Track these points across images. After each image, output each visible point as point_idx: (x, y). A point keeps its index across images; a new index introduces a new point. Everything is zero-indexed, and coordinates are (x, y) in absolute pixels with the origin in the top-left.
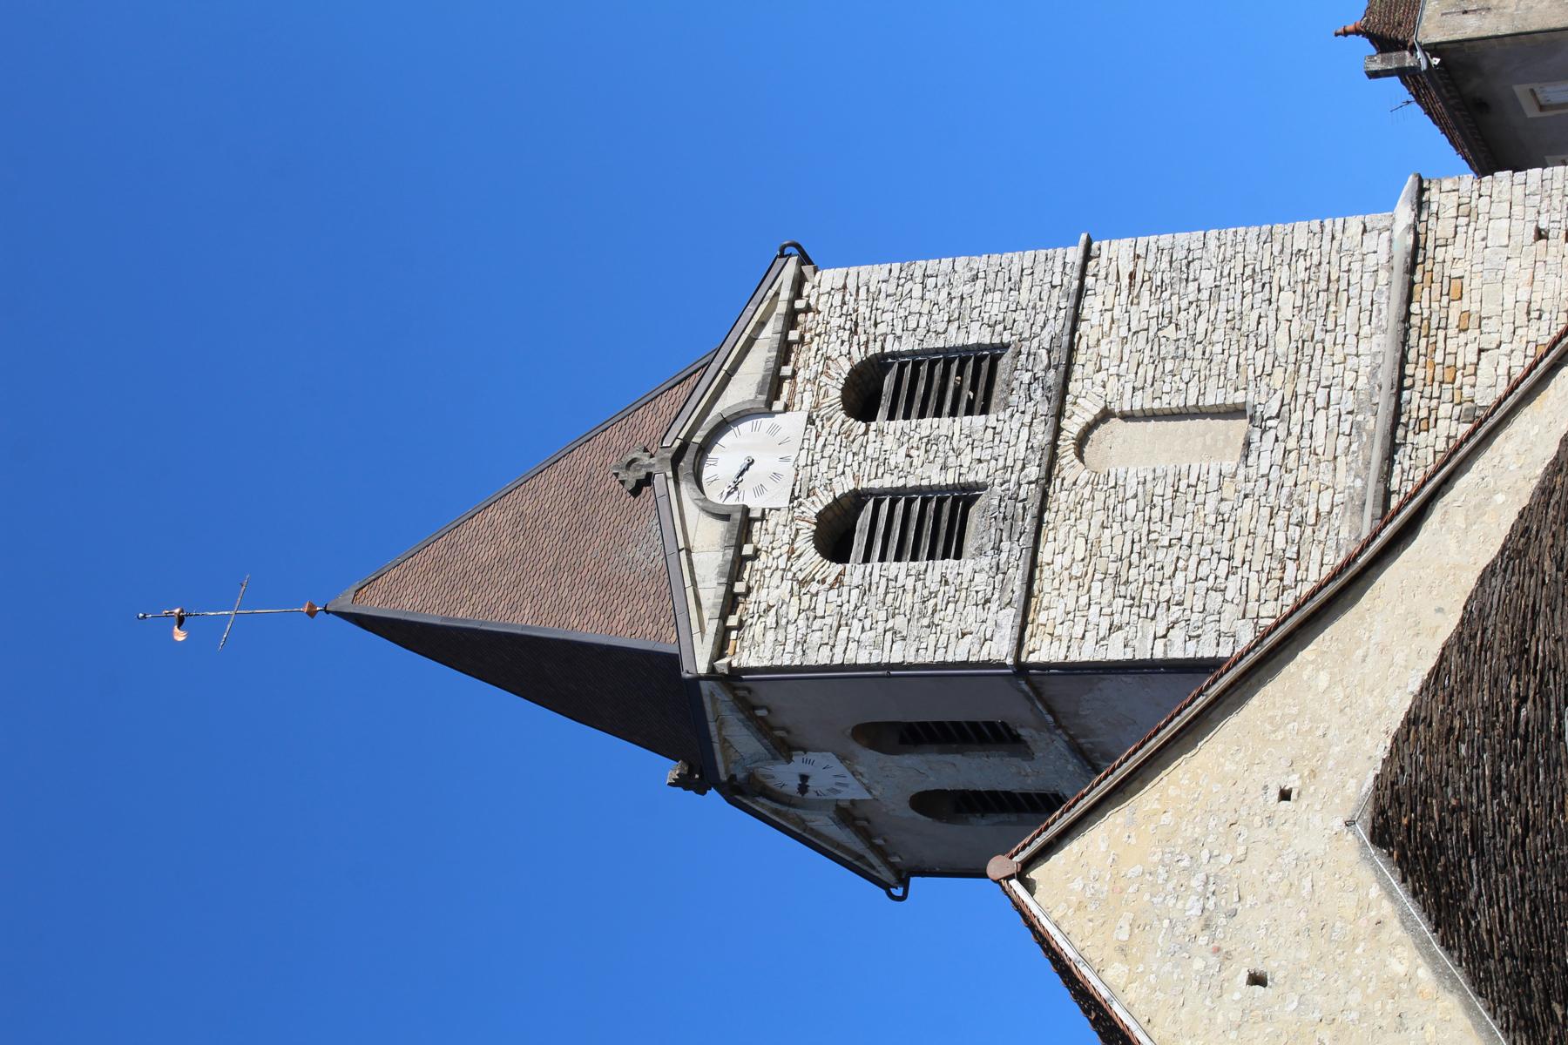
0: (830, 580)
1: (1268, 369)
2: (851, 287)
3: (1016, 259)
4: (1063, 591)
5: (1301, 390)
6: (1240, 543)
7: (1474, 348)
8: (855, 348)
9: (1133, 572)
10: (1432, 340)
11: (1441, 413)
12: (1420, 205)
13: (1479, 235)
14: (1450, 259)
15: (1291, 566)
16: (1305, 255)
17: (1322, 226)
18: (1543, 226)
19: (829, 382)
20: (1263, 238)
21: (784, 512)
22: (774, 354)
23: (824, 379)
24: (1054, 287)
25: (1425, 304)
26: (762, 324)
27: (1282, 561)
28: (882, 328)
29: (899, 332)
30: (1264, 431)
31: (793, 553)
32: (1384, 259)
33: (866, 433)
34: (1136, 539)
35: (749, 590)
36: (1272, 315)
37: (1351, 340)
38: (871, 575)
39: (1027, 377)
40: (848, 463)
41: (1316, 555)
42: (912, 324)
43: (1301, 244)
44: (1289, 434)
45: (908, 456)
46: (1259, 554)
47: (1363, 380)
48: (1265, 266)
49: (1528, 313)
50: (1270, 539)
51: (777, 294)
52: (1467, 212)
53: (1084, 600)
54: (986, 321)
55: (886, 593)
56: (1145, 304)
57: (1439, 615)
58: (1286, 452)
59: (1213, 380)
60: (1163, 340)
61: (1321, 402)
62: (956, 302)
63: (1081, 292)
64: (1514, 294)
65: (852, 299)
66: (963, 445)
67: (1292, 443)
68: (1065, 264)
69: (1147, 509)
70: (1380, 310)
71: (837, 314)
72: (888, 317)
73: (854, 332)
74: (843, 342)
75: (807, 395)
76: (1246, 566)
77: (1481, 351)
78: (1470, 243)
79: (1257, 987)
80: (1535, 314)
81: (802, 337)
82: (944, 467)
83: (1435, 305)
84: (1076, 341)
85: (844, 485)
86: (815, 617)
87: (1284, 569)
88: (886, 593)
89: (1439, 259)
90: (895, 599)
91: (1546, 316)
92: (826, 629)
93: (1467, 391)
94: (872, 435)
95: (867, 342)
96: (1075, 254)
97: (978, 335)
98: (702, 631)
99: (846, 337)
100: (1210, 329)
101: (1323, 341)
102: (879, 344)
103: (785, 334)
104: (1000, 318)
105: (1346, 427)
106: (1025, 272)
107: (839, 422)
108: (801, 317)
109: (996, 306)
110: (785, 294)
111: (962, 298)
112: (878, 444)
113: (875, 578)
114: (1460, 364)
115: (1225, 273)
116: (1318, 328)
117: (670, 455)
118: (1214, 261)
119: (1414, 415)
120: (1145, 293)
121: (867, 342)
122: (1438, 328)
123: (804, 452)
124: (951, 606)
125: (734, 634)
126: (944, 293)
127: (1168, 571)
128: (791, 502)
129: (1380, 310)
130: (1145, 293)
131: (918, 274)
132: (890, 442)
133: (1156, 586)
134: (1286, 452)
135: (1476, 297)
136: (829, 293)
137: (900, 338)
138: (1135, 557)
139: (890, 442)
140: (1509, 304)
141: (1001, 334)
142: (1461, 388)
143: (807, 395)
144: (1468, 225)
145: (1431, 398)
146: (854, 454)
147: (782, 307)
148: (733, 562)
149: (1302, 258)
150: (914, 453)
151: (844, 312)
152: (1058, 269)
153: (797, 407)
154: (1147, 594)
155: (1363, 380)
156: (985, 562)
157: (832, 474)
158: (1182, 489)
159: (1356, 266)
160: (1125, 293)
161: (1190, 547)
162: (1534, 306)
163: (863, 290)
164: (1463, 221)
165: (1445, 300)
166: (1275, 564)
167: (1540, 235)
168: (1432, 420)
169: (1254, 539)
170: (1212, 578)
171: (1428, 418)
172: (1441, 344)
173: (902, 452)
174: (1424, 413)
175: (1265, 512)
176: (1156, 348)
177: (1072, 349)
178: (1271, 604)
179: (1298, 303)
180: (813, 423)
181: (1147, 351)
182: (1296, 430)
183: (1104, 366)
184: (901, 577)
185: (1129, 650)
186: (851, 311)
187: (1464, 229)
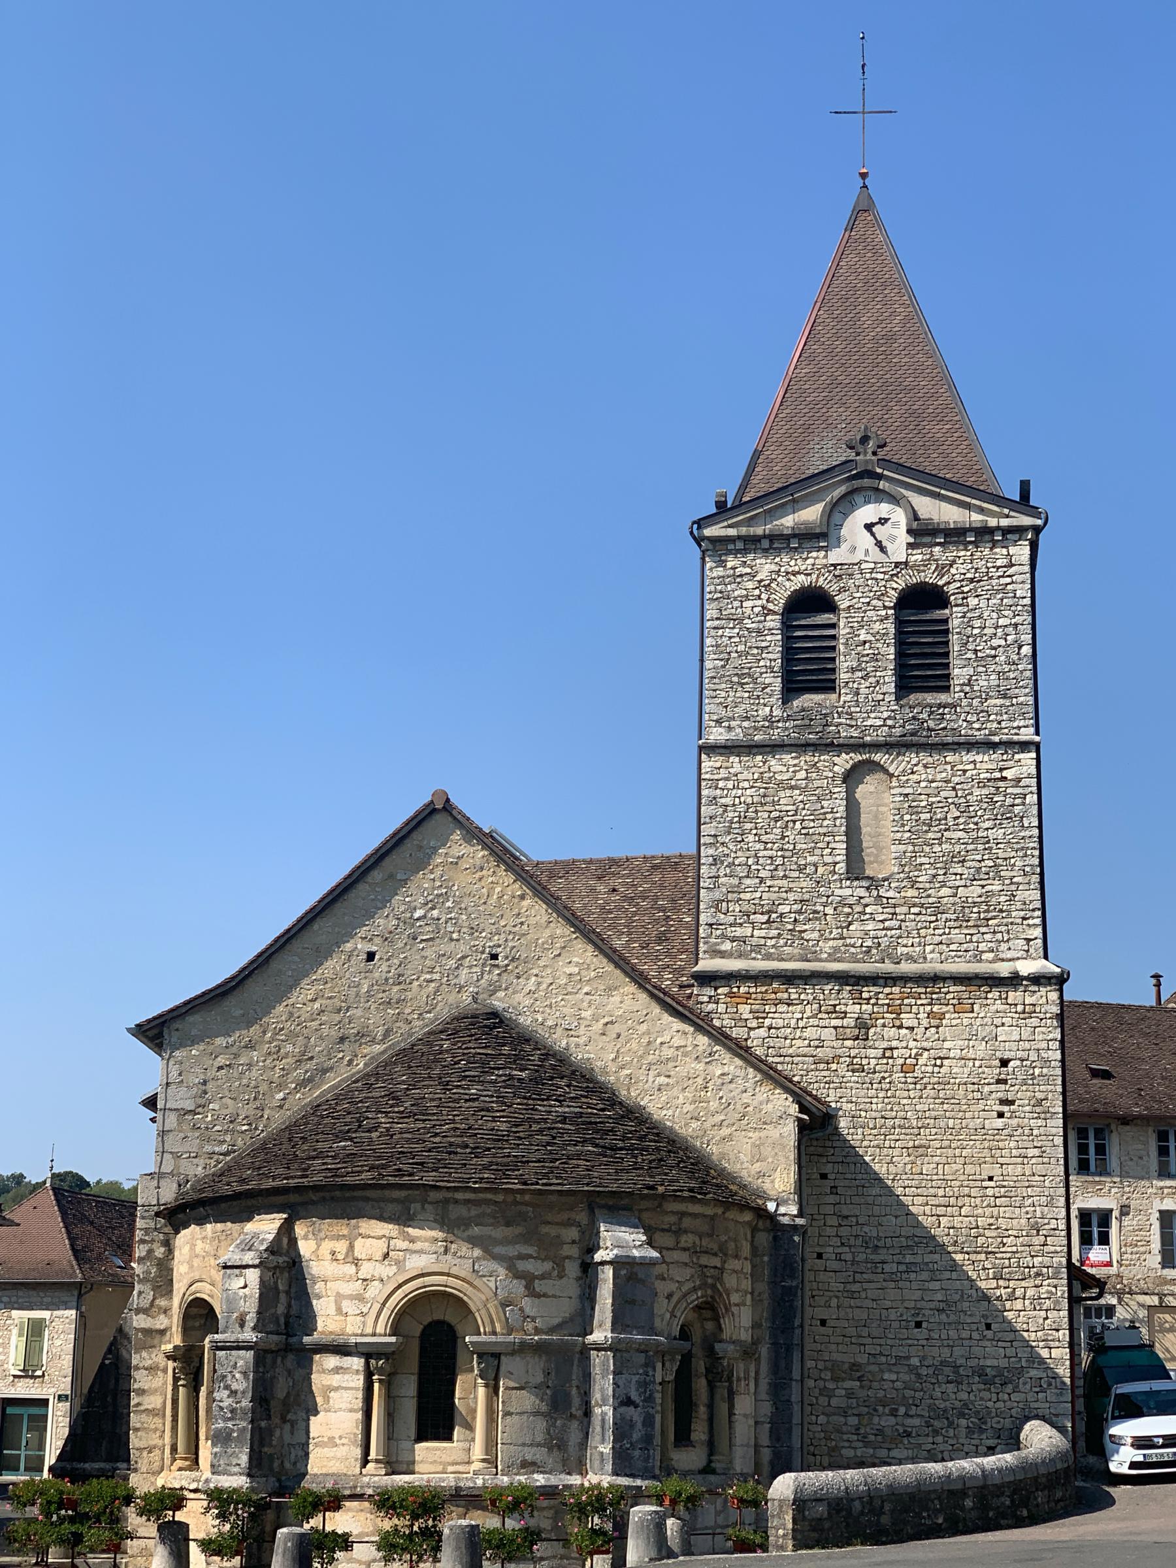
0: (771, 606)
1: (918, 885)
2: (1012, 571)
3: (1027, 690)
4: (754, 769)
5: (898, 910)
6: (784, 883)
7: (915, 1023)
8: (959, 585)
9: (766, 815)
10: (923, 996)
11: (864, 1007)
12: (1038, 980)
13: (1007, 1021)
14: (993, 1002)
15: (765, 918)
16: (1010, 900)
17: (1033, 910)
18: (1011, 1064)
19: (931, 571)
20: (1027, 869)
21: (824, 561)
22: (952, 526)
23: (933, 567)
24: (999, 723)
25: (951, 989)
26: (981, 510)
27: (769, 912)
28: (973, 602)
29: (969, 615)
30: (868, 888)
31: (794, 575)
32: (1001, 956)
33: (885, 607)
34: (789, 813)
35: (765, 551)
36: (963, 883)
37: (937, 939)
38: (772, 634)
39: (925, 716)
40: (861, 600)
41: (774, 933)
42: (977, 623)
43: (1020, 896)
44: (866, 905)
45: (865, 642)
46: (774, 896)
47: (905, 950)
48: (1002, 873)
49: (940, 1058)
50: (787, 902)
51: (1007, 516)
52: (1028, 1012)
53: (746, 785)
54: (974, 678)
55: (757, 648)
56: (977, 792)
57: (615, 1036)
58: (850, 906)
59: (910, 848)
60: (946, 809)
61: (887, 924)
62: (993, 652)
63: (994, 746)
64: (953, 1046)
65: (1002, 574)
66: (870, 680)
67: (858, 909)
68: (1019, 728)
69: (812, 817)
70: (960, 957)
71: (989, 565)
72: (983, 604)
73: (972, 580)
74: (965, 574)
75: (920, 557)
76: (767, 889)
77: (912, 1029)
78: (1001, 1015)
79: (365, 957)
80: (939, 1062)
81: (971, 542)
82: (853, 670)
83: (951, 996)
84: (950, 747)
85: (843, 601)
86: (741, 601)
87: (762, 914)
88: (757, 648)
89: (990, 996)
90: (753, 655)
91: (936, 1069)
92: (733, 611)
93: (882, 1021)
94: (883, 613)
95: (963, 592)
96: (1027, 734)
97: (959, 673)
98: (729, 526)
99: (969, 576)
100: (953, 841)
101: (937, 920)
102: (960, 602)
103: (971, 529)
104: (976, 688)
105: (869, 943)
106: (1014, 700)
107: (895, 586)
108: (987, 537)
109: (985, 683)
110: (1005, 522)
111: (995, 656)
112: (875, 619)
113: (768, 638)
114: (902, 1016)
115: (999, 846)
116: (948, 916)
117: (870, 468)
118: (1011, 836)
119: (865, 989)
120: (985, 791)
121: (963, 592)
122: (932, 999)
123: (872, 565)
124: (746, 695)
125: (731, 547)
126: (1003, 642)
127: (764, 838)
128: (832, 565)
129: (960, 957)
130: (985, 791)
131: (1018, 619)
132: (877, 626)
133: (754, 832)
134: (850, 906)
135: (954, 1022)
136: (1009, 555)
137: (964, 617)
138: (777, 814)
139: (877, 626)
140: (947, 1045)
141: (961, 691)
142: (883, 1018)
143: (920, 557)
144: (1016, 1012)
145: (877, 999)
146: (868, 603)
147: (993, 522)
148: (782, 535)
149: (1008, 898)
150: (867, 645)
151: (991, 570)
152: (1015, 724)
153: (910, 551)
154: (748, 826)
155: (905, 950)
156: (777, 712)
157: (853, 589)
158: (827, 839)
159: (999, 936)
160: (988, 775)
161: (782, 850)
162: (946, 1062)
163: (1008, 580)
164: (1020, 1008)
165: (955, 1002)
166: (766, 908)
167: (1004, 1063)
168: (861, 1001)
169: (786, 892)
170: (760, 867)
171: (861, 998)
172: (919, 1002)
173: (869, 637)
174: (865, 995)
175: (806, 897)
176: (940, 805)
177: (943, 747)
178: (737, 910)
179: (970, 900)
180: (896, 567)
181: (938, 799)
182: (868, 910)
183: (929, 770)
184: (771, 656)
185: (708, 820)
186: (990, 575)
187: (1014, 1010)
